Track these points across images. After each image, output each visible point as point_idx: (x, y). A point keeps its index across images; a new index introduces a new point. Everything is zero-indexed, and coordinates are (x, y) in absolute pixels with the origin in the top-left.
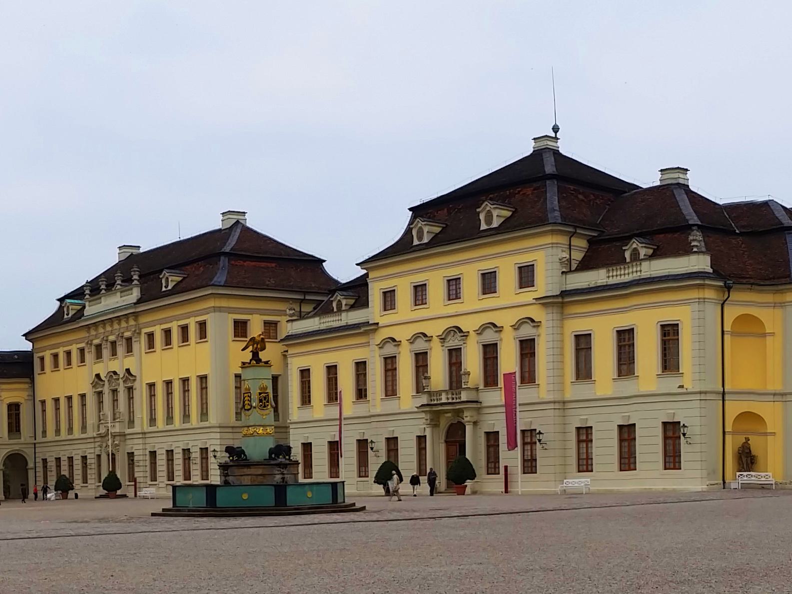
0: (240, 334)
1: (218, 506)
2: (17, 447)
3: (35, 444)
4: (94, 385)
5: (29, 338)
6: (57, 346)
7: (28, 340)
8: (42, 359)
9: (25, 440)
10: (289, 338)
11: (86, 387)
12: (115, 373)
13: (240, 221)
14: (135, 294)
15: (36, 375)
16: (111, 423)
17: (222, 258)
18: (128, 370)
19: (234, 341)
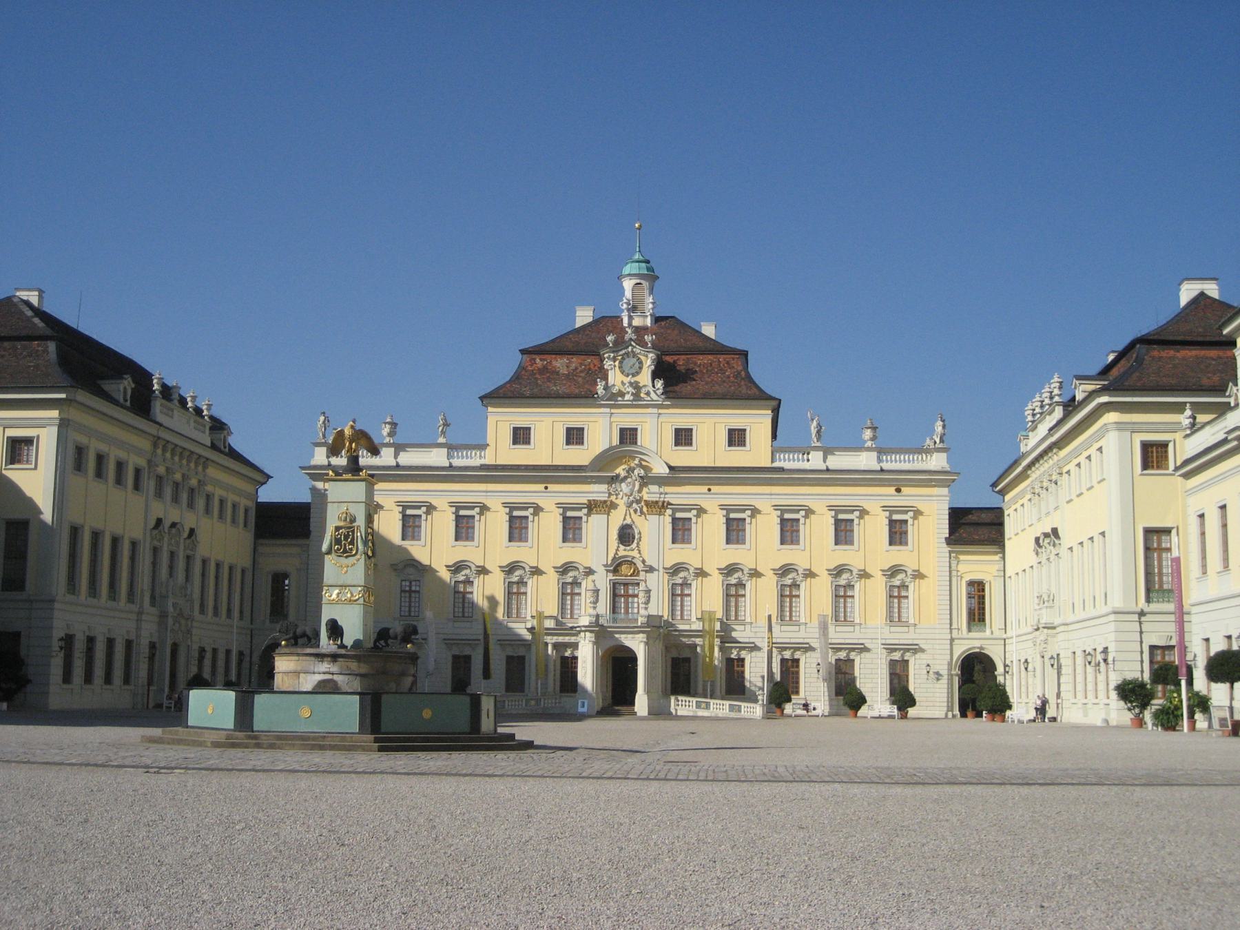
0: (1155, 464)
1: (189, 724)
2: (977, 644)
3: (1005, 640)
4: (1037, 554)
5: (998, 488)
6: (1014, 500)
7: (997, 492)
8: (1009, 515)
9: (992, 633)
10: (1187, 462)
11: (1033, 560)
12: (1046, 535)
13: (1206, 292)
14: (1058, 413)
15: (1006, 541)
16: (637, 596)
17: (1138, 346)
18: (1055, 531)
19: (1141, 475)
